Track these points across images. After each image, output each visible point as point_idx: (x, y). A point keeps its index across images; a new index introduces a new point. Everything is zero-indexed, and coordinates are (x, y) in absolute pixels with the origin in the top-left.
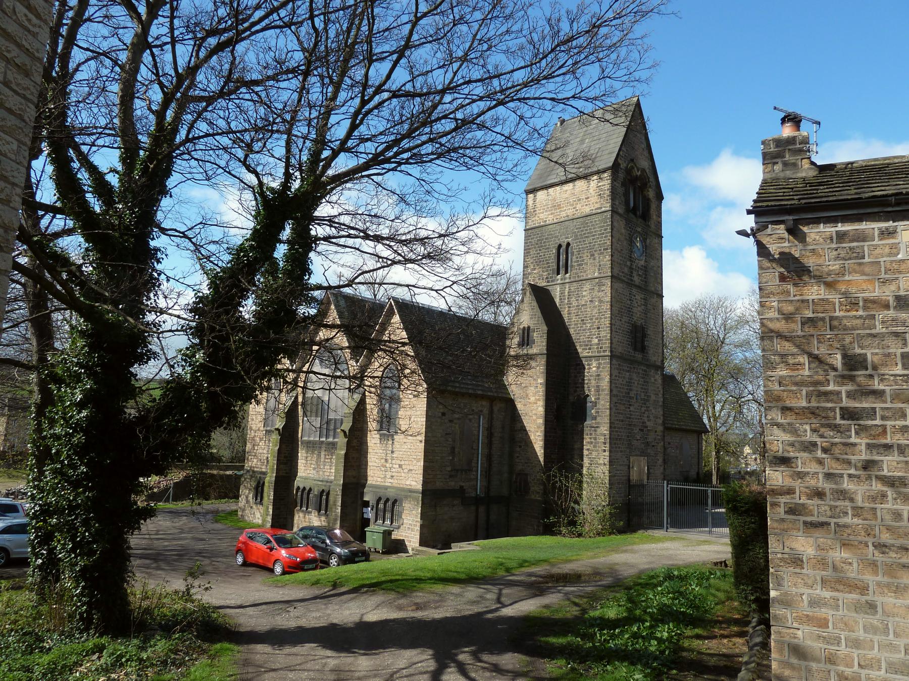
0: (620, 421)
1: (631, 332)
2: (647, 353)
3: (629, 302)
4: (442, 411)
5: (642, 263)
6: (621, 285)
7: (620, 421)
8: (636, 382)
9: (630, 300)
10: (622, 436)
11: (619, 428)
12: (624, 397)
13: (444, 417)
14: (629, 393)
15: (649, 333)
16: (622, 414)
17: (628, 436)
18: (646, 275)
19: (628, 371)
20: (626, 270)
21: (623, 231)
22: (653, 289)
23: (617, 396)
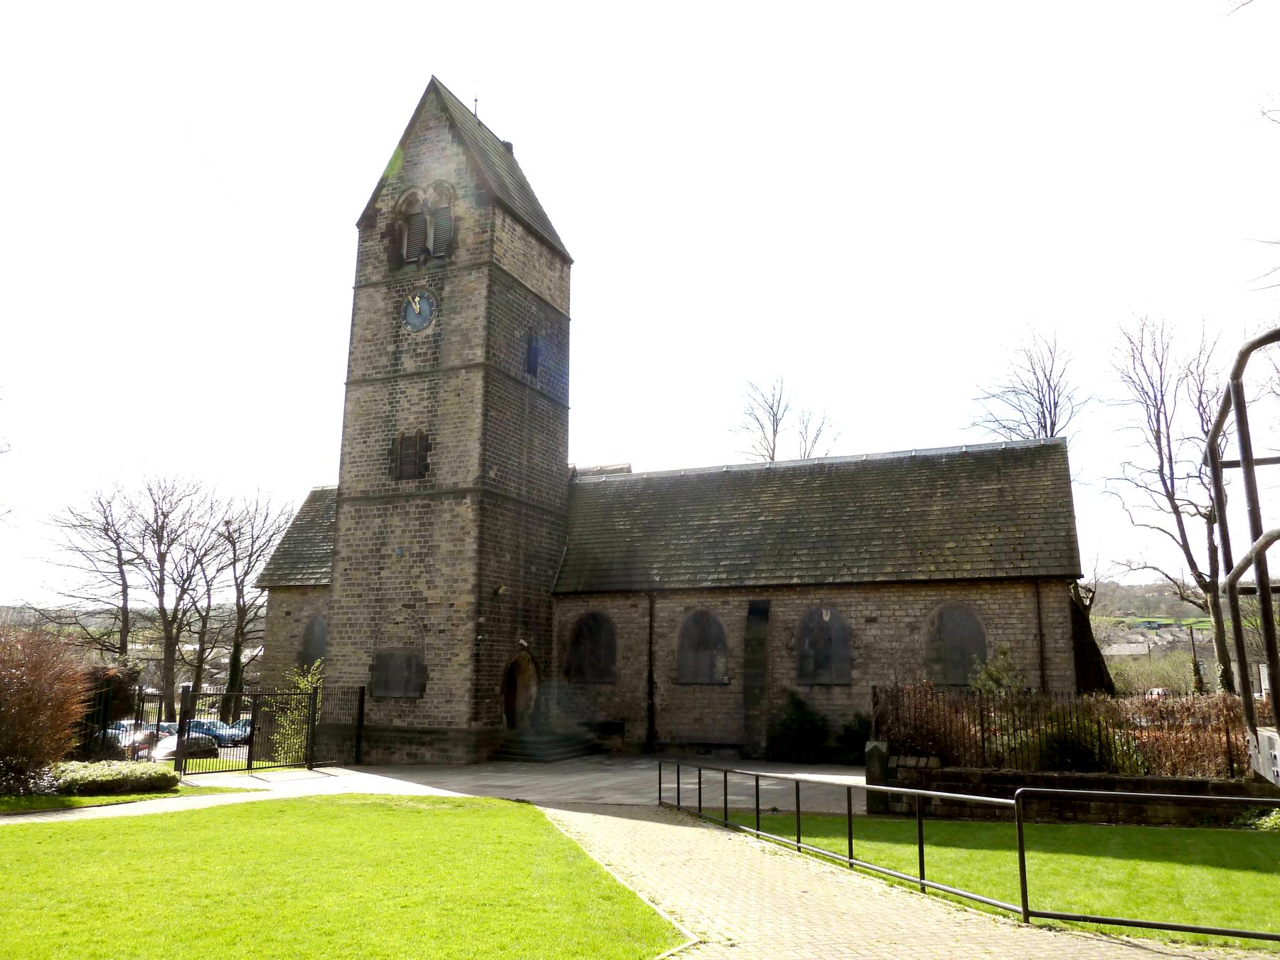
0: (353, 596)
1: (391, 452)
2: (435, 475)
3: (388, 408)
4: (285, 610)
5: (429, 331)
6: (370, 389)
7: (353, 596)
8: (398, 531)
9: (390, 403)
10: (357, 619)
11: (351, 607)
13: (288, 617)
15: (439, 440)
16: (359, 585)
18: (437, 347)
19: (380, 516)
20: (384, 361)
21: (381, 304)
22: (457, 362)
23: (349, 558)
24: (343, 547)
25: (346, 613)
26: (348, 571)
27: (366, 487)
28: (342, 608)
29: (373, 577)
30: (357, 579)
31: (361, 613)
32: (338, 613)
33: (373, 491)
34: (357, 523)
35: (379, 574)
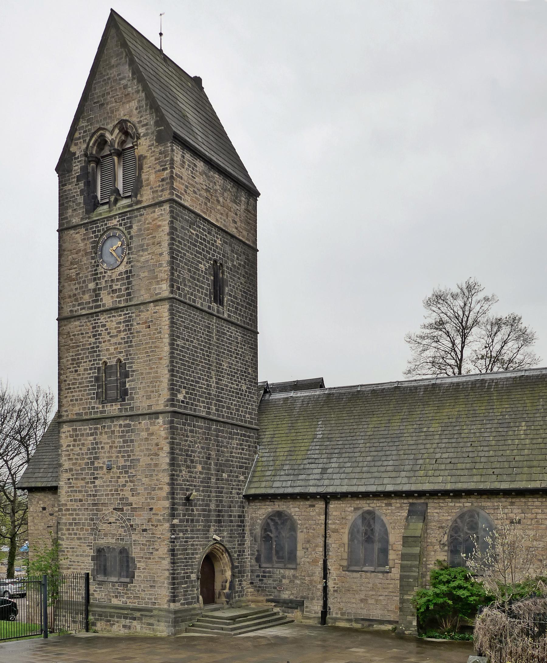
0: (76, 500)
7: (76, 500)
8: (107, 447)
10: (79, 519)
11: (75, 510)
12: (82, 469)
14: (93, 463)
17: (92, 520)
19: (92, 435)
23: (71, 470)
24: (65, 460)
25: (72, 514)
26: (71, 481)
27: (80, 410)
28: (68, 510)
29: (90, 485)
30: (78, 487)
31: (83, 514)
32: (65, 515)
33: (86, 414)
34: (75, 440)
35: (94, 482)
